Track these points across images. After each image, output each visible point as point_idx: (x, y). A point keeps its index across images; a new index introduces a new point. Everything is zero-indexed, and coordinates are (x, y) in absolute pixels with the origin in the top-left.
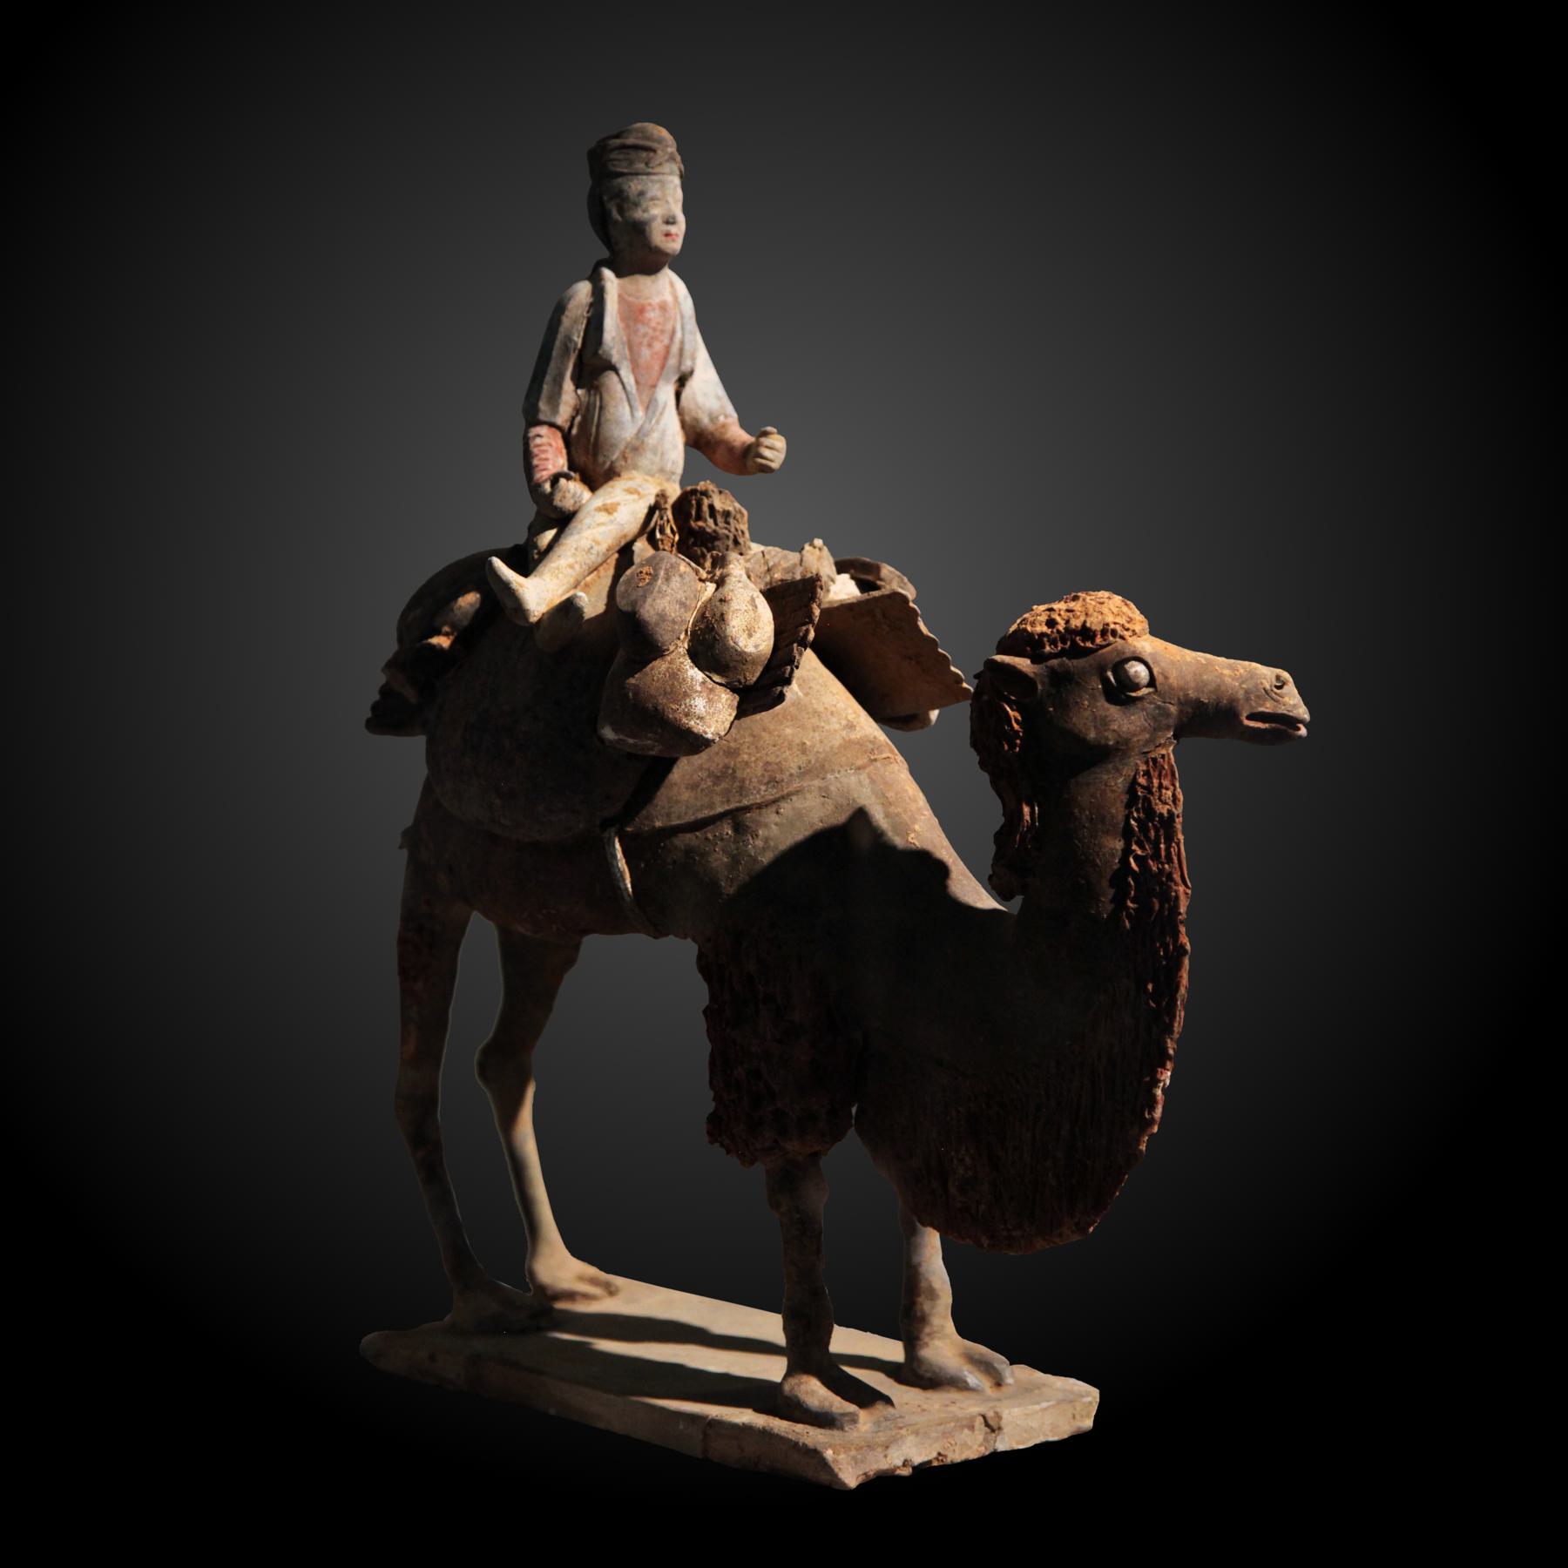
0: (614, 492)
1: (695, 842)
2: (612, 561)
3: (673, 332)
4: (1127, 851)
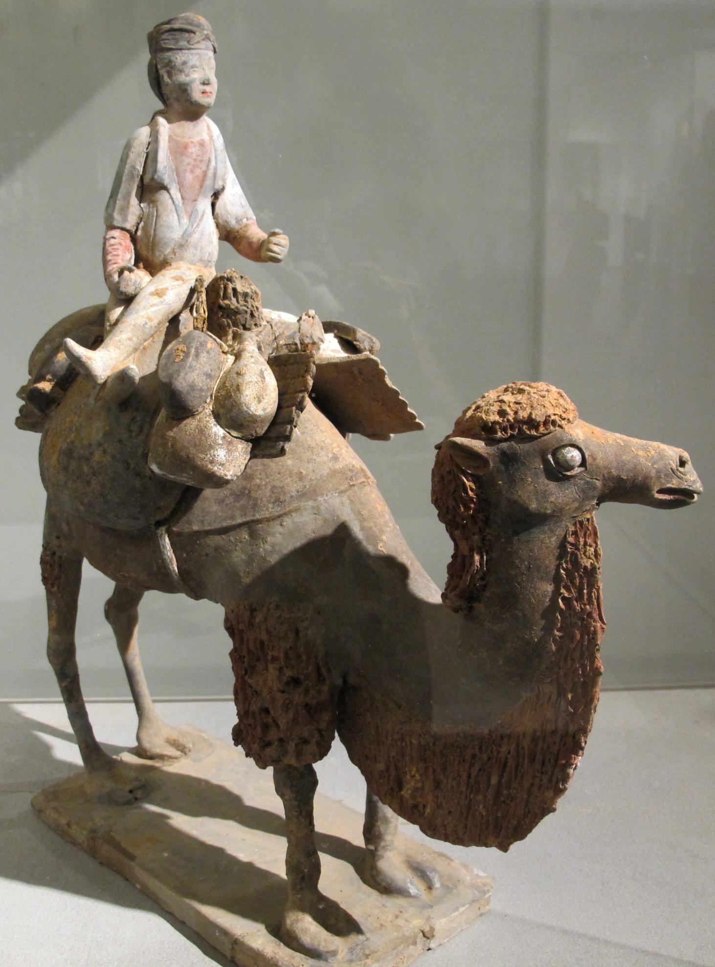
0: (166, 278)
1: (222, 543)
2: (164, 330)
3: (209, 161)
4: (556, 593)
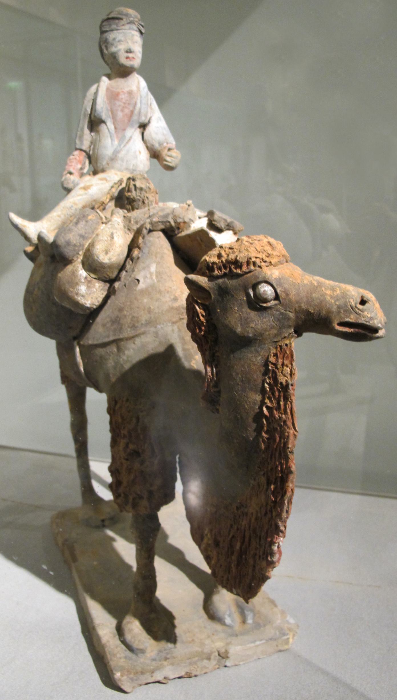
1: (103, 353)
3: (136, 104)
4: (263, 403)
